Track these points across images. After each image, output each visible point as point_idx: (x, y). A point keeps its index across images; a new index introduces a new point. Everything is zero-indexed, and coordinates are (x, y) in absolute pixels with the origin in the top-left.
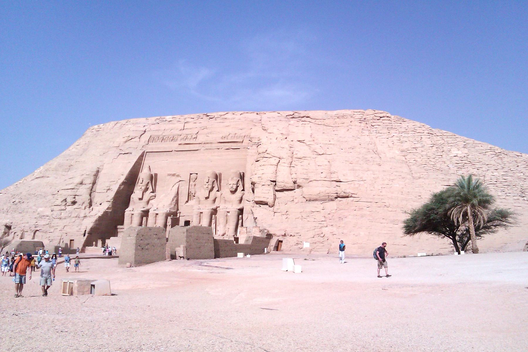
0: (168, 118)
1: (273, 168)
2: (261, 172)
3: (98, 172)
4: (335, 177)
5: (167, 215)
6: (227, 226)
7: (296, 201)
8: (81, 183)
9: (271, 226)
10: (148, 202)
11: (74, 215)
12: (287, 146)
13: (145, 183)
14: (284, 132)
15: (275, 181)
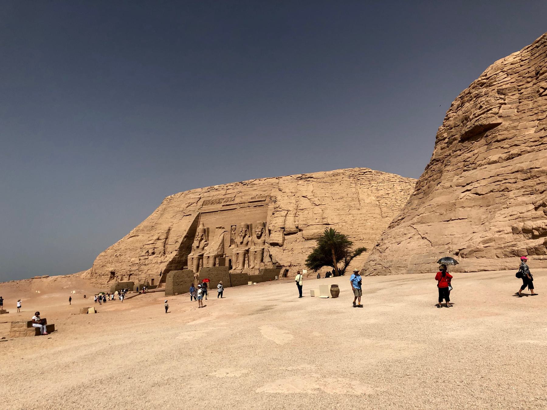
0: (216, 187)
1: (283, 218)
2: (274, 222)
3: (169, 230)
4: (325, 221)
5: (215, 257)
6: (256, 262)
7: (298, 240)
8: (158, 239)
9: (281, 260)
10: (203, 249)
11: (154, 261)
12: (294, 201)
13: (200, 234)
14: (293, 191)
15: (284, 228)
